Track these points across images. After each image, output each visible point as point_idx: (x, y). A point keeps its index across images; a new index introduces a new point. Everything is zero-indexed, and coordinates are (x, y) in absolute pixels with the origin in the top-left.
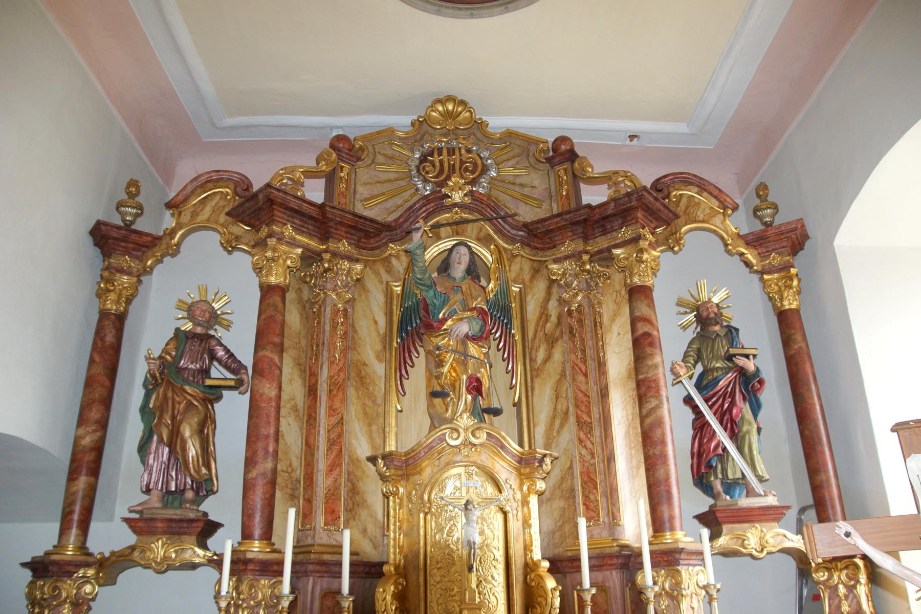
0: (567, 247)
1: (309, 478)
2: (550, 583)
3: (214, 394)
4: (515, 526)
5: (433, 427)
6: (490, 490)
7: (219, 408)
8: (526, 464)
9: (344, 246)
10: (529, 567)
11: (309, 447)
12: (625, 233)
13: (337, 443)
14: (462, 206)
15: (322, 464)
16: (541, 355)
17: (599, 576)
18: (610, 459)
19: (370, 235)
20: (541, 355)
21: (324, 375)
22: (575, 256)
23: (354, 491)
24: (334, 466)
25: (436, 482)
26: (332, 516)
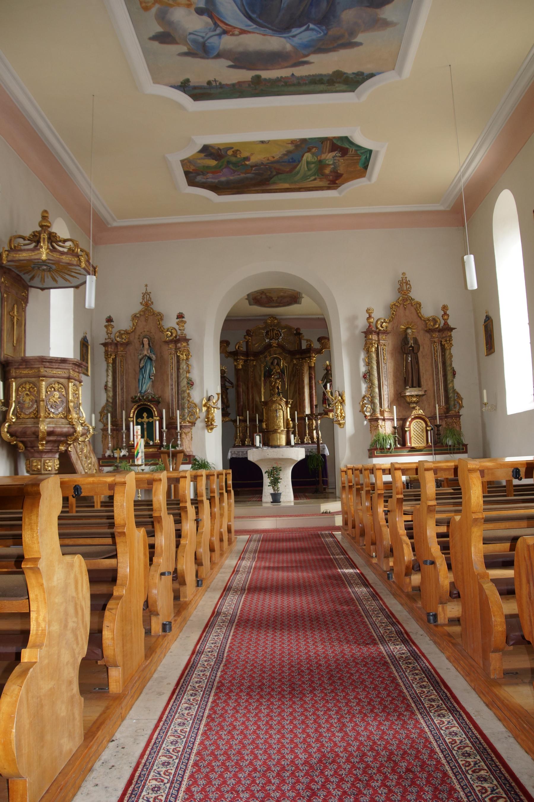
0: (297, 356)
1: (248, 405)
2: (291, 422)
3: (228, 389)
4: (285, 413)
5: (271, 396)
6: (280, 407)
7: (228, 391)
8: (287, 403)
9: (252, 358)
10: (287, 419)
11: (248, 399)
12: (308, 355)
13: (253, 398)
14: (275, 347)
15: (251, 402)
16: (292, 379)
17: (300, 421)
18: (303, 400)
19: (256, 355)
20: (292, 379)
21: (250, 385)
22: (298, 359)
23: (257, 407)
24: (253, 402)
25: (271, 406)
26: (253, 412)
